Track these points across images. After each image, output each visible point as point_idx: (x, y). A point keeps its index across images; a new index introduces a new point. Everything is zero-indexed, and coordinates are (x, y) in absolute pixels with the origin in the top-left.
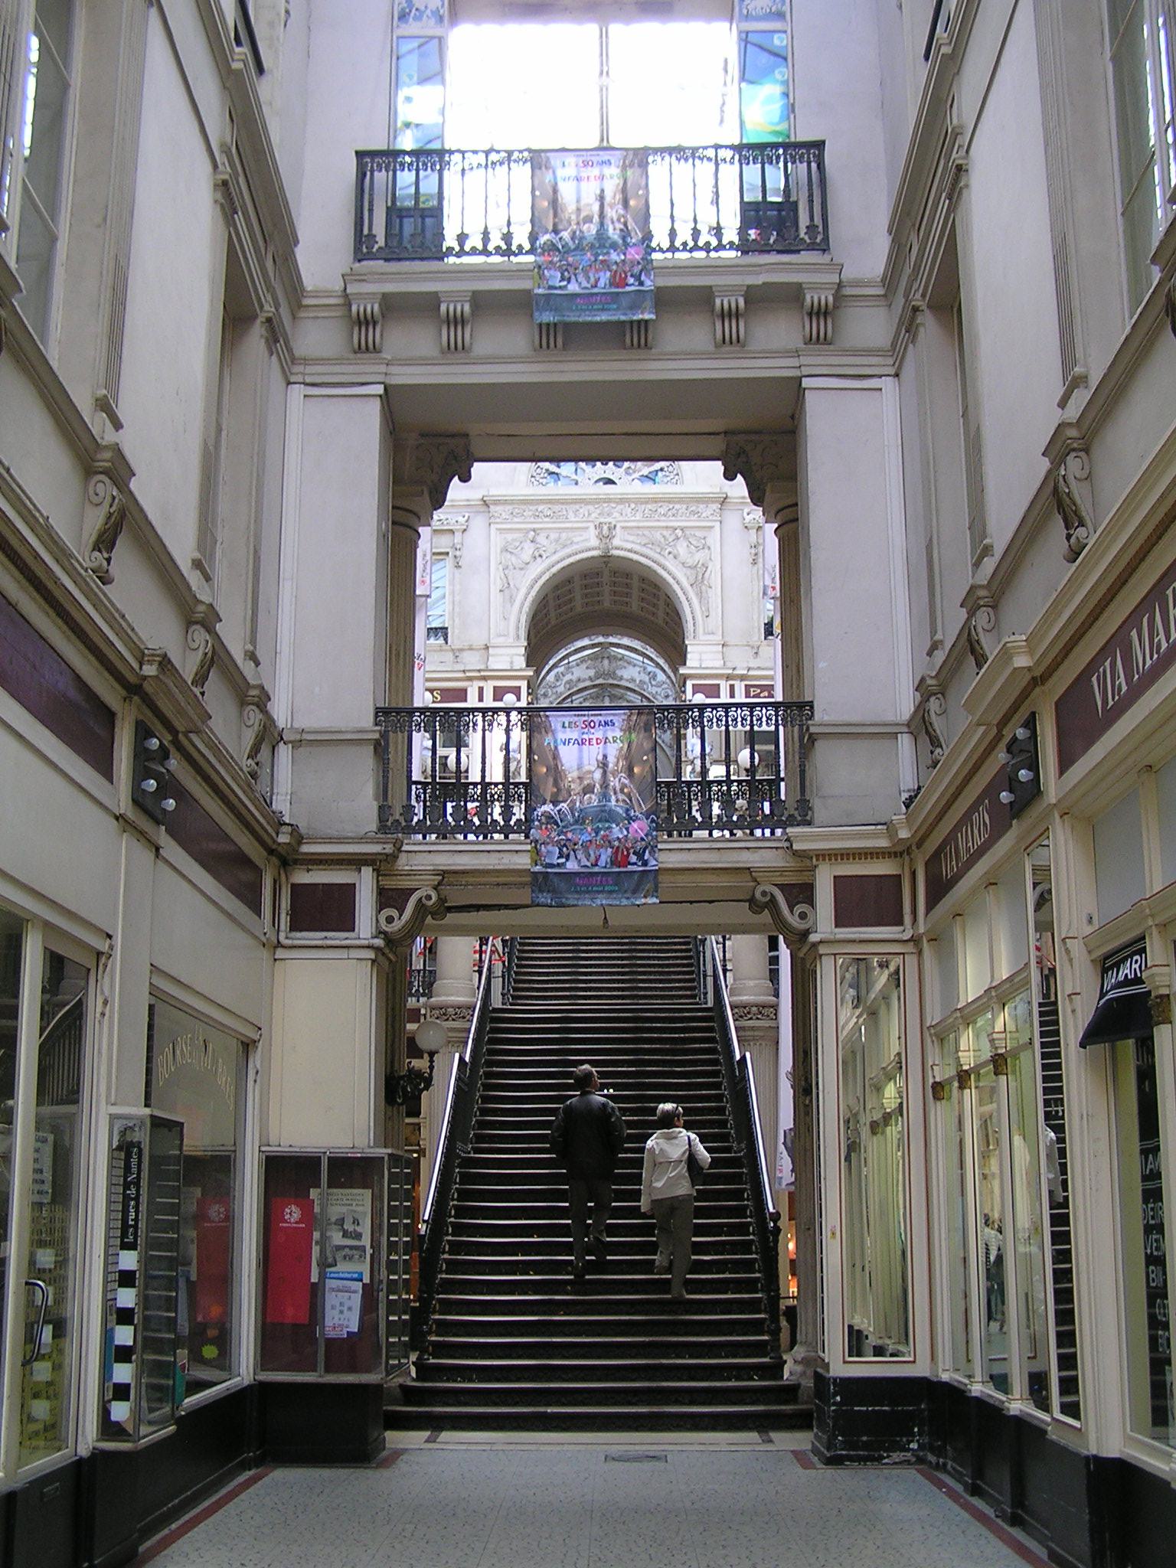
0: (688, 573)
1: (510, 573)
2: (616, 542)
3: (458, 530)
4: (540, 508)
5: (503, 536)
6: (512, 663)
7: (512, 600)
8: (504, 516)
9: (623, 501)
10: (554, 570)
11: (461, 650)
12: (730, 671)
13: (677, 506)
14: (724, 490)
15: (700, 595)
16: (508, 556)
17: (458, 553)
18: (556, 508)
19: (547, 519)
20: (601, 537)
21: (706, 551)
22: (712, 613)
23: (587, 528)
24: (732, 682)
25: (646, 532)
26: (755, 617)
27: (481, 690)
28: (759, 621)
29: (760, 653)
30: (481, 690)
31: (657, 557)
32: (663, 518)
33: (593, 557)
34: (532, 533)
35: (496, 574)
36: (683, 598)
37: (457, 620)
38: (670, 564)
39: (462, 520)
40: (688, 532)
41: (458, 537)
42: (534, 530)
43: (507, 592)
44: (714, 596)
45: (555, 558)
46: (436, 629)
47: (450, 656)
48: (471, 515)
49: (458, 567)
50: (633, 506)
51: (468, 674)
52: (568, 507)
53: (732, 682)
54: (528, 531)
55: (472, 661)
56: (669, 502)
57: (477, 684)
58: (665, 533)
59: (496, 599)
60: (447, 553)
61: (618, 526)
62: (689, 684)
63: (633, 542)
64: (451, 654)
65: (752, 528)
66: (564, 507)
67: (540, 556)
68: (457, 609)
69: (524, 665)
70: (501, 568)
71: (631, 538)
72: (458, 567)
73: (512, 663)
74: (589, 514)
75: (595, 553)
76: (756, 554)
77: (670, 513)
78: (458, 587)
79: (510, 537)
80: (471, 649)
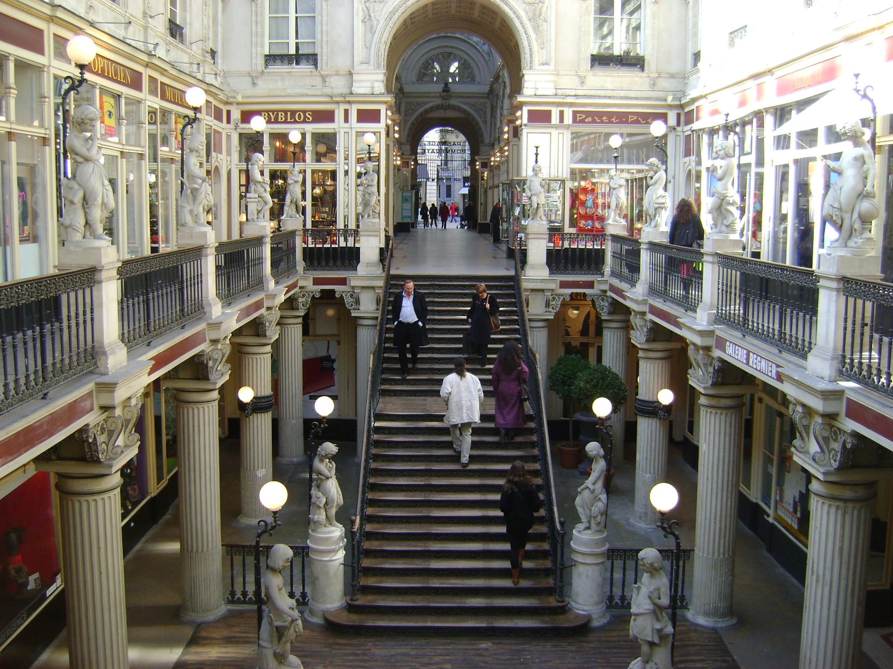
0: (527, 8)
15: (536, 28)
24: (562, 109)
27: (346, 112)
30: (346, 112)
36: (522, 31)
37: (325, 49)
43: (368, 24)
47: (318, 81)
53: (562, 109)
55: (338, 85)
57: (343, 107)
62: (525, 109)
64: (320, 79)
68: (325, 39)
69: (383, 90)
73: (373, 88)
80: (337, 74)
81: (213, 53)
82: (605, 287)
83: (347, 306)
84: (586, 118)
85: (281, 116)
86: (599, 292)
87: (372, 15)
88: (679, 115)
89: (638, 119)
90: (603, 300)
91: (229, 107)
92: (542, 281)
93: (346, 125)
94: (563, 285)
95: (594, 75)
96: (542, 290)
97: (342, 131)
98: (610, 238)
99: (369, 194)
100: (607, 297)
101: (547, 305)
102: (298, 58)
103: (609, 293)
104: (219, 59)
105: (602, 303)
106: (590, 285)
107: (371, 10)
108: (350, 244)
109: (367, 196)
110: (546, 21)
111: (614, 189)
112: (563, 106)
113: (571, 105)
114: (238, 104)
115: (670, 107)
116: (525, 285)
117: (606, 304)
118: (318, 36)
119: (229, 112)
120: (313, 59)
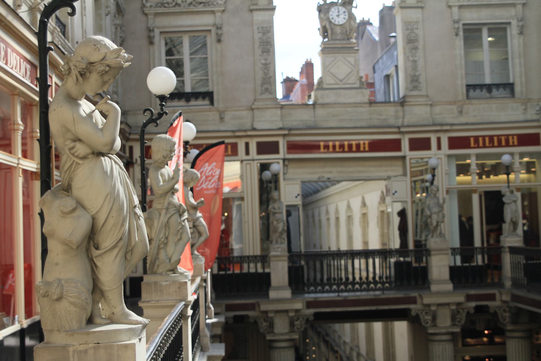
3: (218, 11)
72: (219, 41)
83: (261, 331)
96: (448, 304)
98: (507, 250)
99: (277, 221)
101: (453, 318)
102: (196, 95)
106: (492, 297)
108: (260, 270)
109: (275, 223)
111: (508, 204)
117: (507, 314)
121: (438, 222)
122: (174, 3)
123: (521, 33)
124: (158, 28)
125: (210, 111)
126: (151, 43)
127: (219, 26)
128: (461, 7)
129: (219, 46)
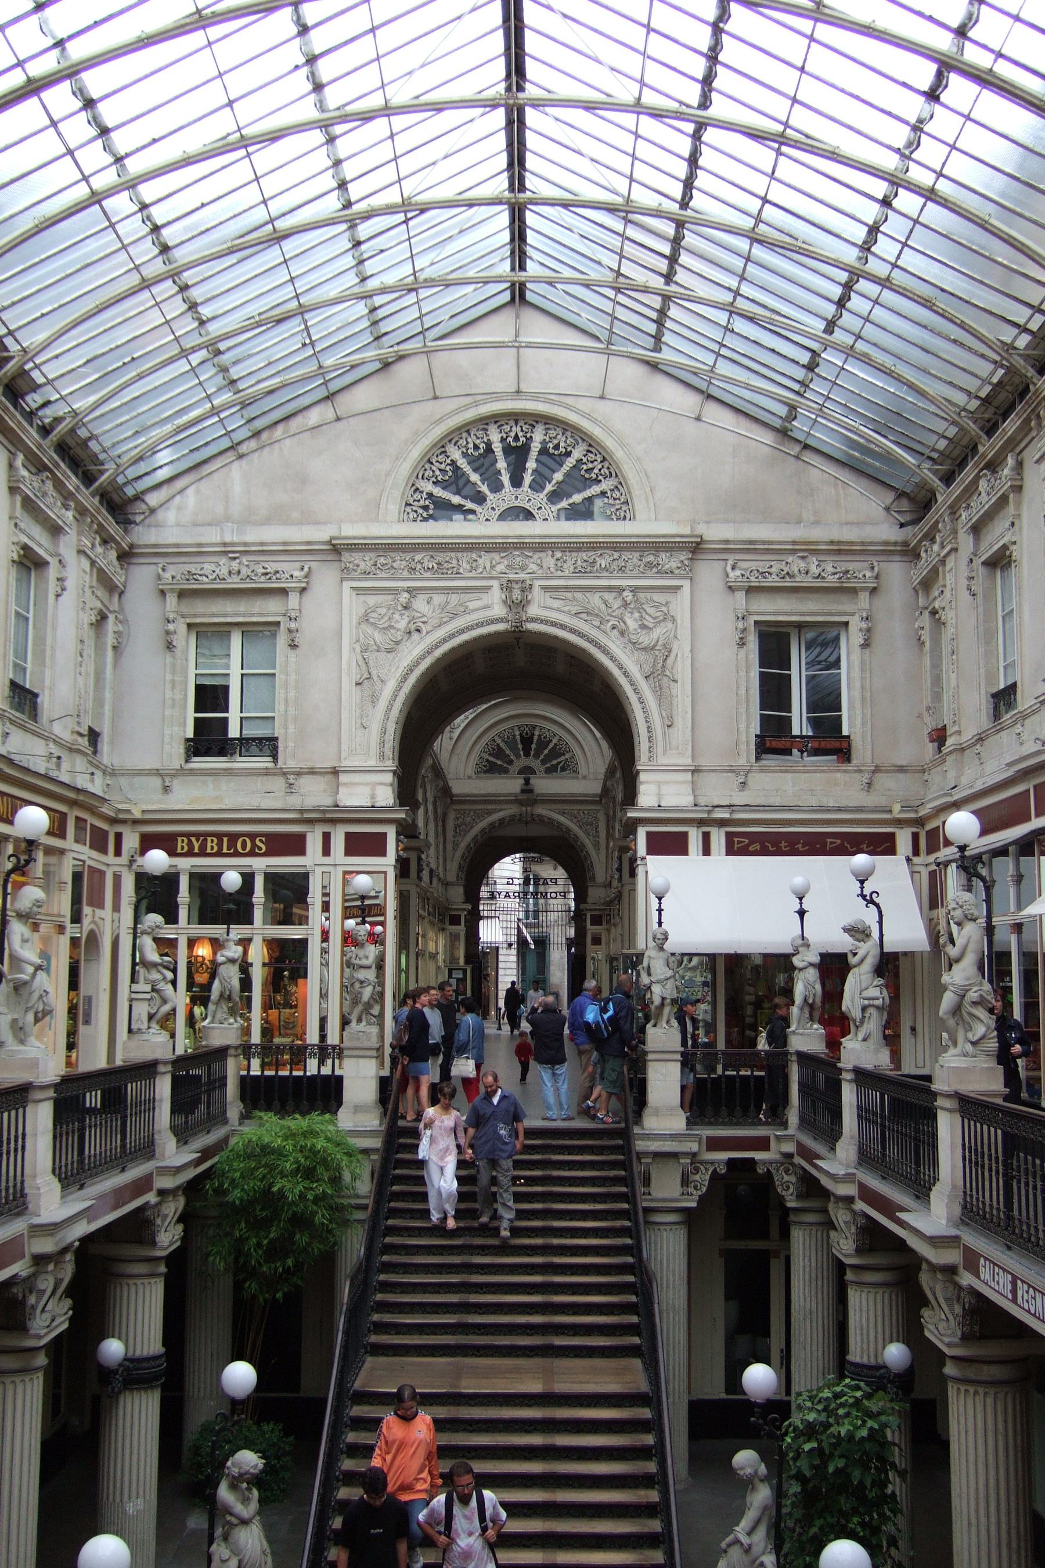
1: (372, 657)
2: (533, 610)
3: (293, 589)
4: (418, 557)
5: (362, 598)
6: (373, 797)
7: (374, 700)
8: (362, 565)
9: (542, 546)
10: (438, 653)
11: (299, 774)
12: (705, 815)
13: (626, 555)
14: (698, 532)
16: (370, 630)
17: (293, 625)
18: (440, 557)
19: (428, 575)
20: (511, 605)
21: (670, 625)
22: (679, 721)
23: (489, 588)
24: (706, 829)
25: (578, 595)
26: (742, 726)
27: (327, 838)
28: (747, 733)
29: (750, 782)
30: (327, 838)
31: (594, 633)
32: (606, 574)
33: (497, 634)
34: (406, 595)
35: (349, 656)
37: (291, 729)
38: (615, 645)
39: (296, 574)
40: (641, 595)
41: (293, 599)
42: (409, 591)
44: (682, 694)
45: (441, 633)
46: (261, 739)
48: (314, 565)
49: (293, 646)
50: (558, 555)
51: (306, 816)
52: (459, 555)
54: (395, 591)
56: (615, 549)
58: (609, 596)
59: (350, 695)
60: (278, 624)
61: (537, 583)
62: (642, 834)
63: (559, 610)
65: (739, 589)
66: (453, 554)
67: (418, 631)
68: (291, 711)
70: (358, 650)
71: (556, 604)
72: (293, 646)
73: (373, 797)
74: (493, 567)
75: (501, 627)
76: (744, 630)
77: (614, 566)
78: (293, 677)
79: (372, 600)
80: (313, 773)
81: (94, 736)
82: (789, 1148)
84: (751, 843)
85: (211, 845)
86: (778, 1157)
87: (374, 673)
88: (915, 837)
89: (842, 845)
90: (787, 1171)
91: (119, 828)
92: (673, 1137)
93: (326, 860)
94: (714, 1144)
95: (762, 771)
96: (674, 1155)
97: (319, 871)
98: (794, 1058)
100: (793, 1164)
101: (685, 1181)
102: (245, 745)
103: (797, 1160)
104: (104, 745)
105: (786, 1178)
106: (763, 1144)
107: (371, 664)
110: (675, 681)
111: (801, 970)
112: (709, 825)
113: (722, 823)
114: (136, 822)
115: (900, 823)
116: (640, 1145)
118: (280, 707)
119: (119, 837)
120: (269, 745)
121: (663, 999)
122: (215, 575)
123: (866, 645)
124: (183, 617)
125: (266, 772)
126: (170, 646)
127: (293, 615)
128: (750, 590)
129: (292, 655)
